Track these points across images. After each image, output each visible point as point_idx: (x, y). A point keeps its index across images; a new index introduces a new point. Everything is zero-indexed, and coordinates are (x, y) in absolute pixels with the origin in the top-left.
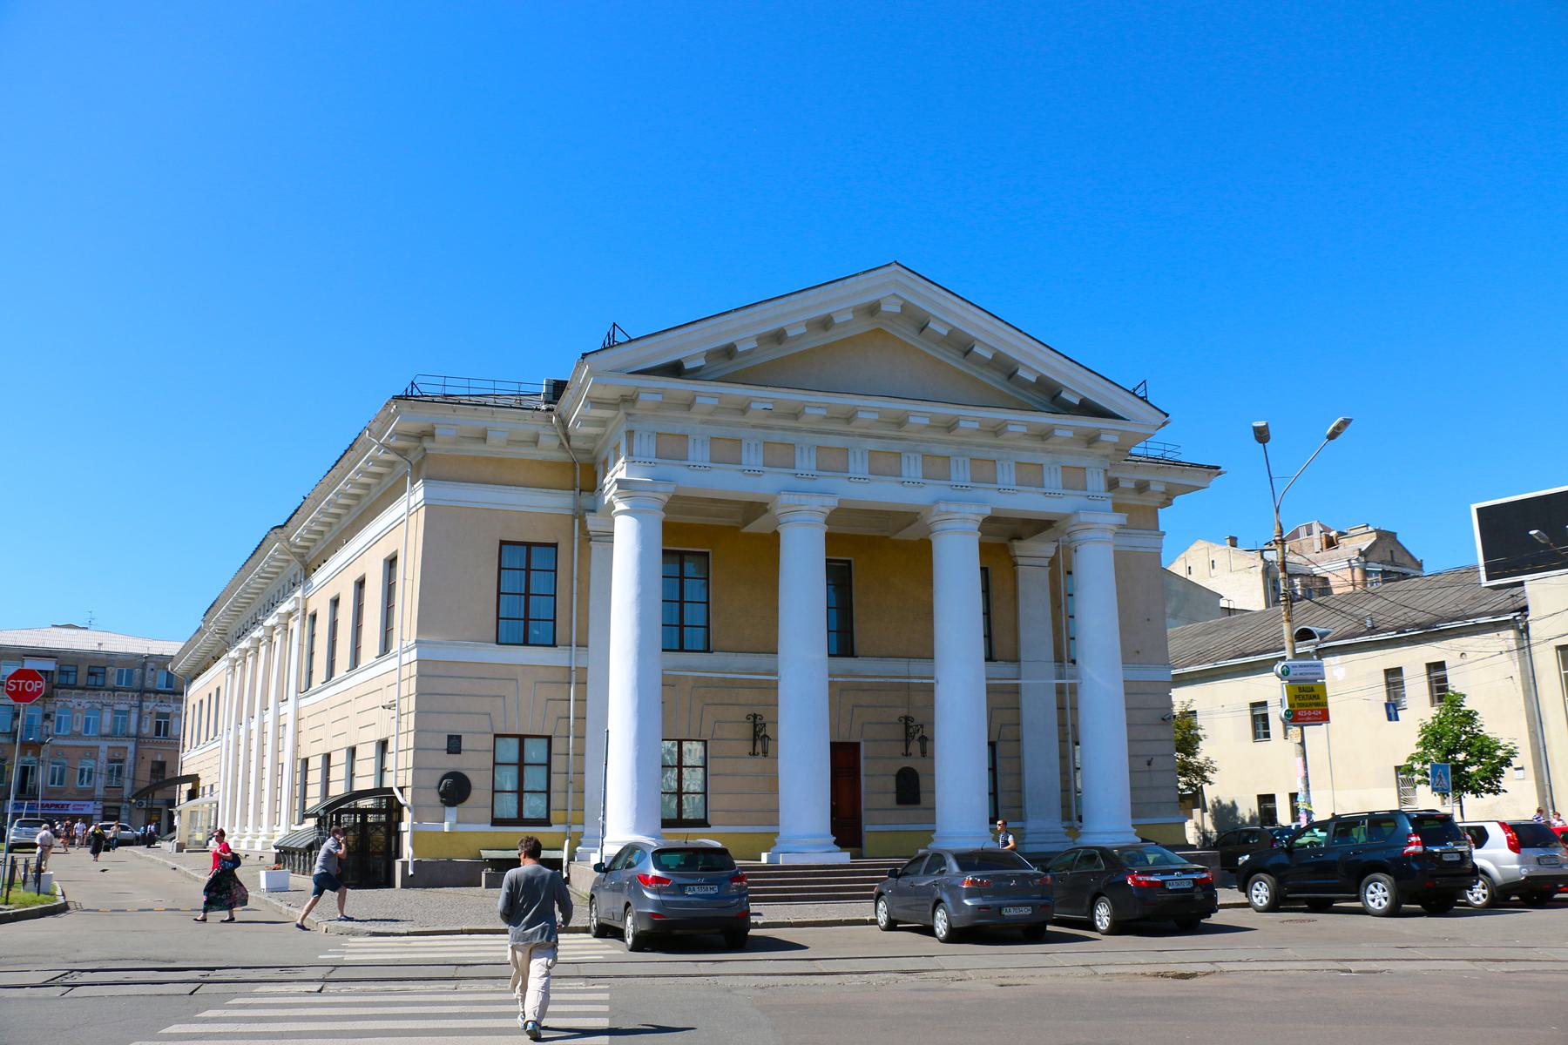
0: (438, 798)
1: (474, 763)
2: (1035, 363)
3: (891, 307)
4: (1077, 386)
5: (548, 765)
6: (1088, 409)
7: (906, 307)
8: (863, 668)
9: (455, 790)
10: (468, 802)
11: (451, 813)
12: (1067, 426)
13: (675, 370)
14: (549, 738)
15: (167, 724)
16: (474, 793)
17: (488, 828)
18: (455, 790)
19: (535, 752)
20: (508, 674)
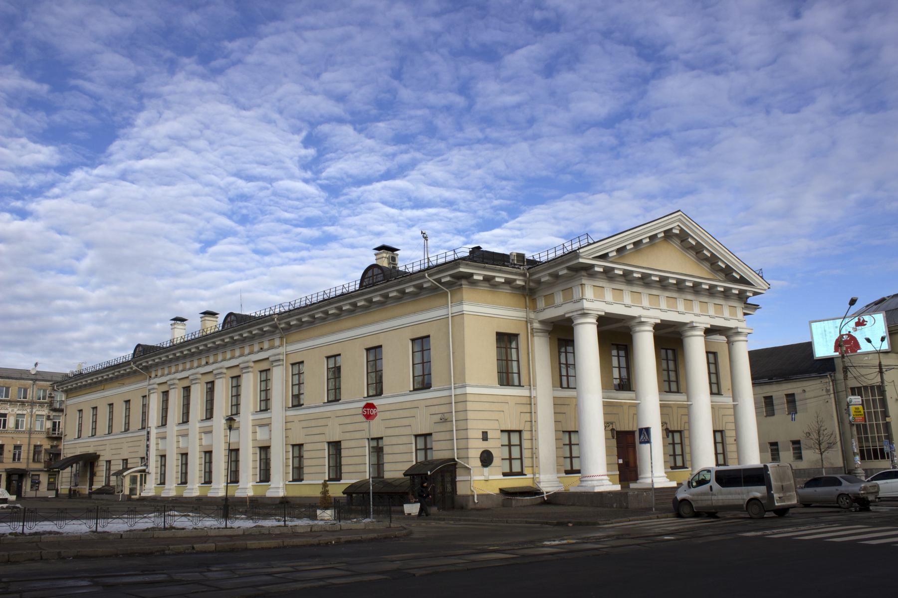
0: (480, 464)
1: (495, 445)
2: (727, 259)
3: (676, 231)
4: (741, 270)
5: (520, 445)
6: (743, 281)
7: (682, 230)
8: (717, 399)
9: (486, 459)
10: (493, 464)
11: (486, 469)
12: (736, 288)
13: (604, 257)
14: (520, 432)
15: (5, 421)
16: (495, 459)
17: (501, 477)
18: (486, 459)
19: (515, 439)
20: (504, 400)
